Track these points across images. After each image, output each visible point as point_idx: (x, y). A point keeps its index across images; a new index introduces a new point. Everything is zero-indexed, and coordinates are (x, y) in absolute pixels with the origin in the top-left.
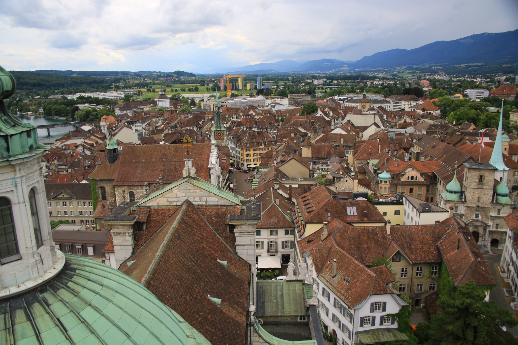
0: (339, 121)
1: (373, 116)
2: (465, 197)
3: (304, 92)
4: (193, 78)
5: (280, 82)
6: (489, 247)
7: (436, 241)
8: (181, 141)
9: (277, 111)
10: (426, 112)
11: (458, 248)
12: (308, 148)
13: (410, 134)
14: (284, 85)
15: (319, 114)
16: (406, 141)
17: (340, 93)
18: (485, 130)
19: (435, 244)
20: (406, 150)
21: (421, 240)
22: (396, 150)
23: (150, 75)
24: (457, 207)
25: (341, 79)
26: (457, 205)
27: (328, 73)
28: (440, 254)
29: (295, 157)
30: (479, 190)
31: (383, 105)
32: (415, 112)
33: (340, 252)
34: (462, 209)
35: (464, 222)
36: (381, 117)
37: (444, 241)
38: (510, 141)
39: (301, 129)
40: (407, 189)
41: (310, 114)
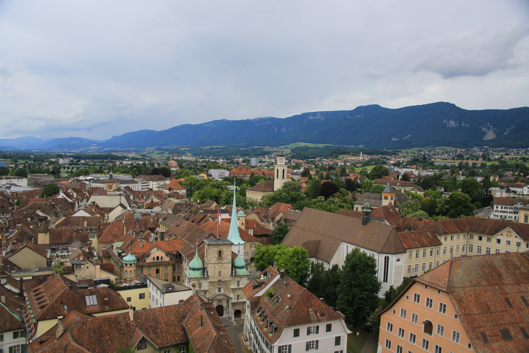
0: (83, 203)
1: (119, 197)
2: (207, 273)
3: (47, 171)
5: (20, 160)
6: (233, 319)
7: (181, 321)
9: (13, 193)
10: (172, 191)
11: (202, 325)
12: (45, 234)
13: (156, 214)
14: (24, 164)
15: (61, 195)
16: (152, 221)
17: (86, 173)
18: (225, 207)
19: (180, 324)
20: (152, 230)
21: (166, 322)
22: (142, 231)
24: (200, 284)
25: (89, 159)
26: (200, 282)
27: (75, 151)
28: (185, 335)
29: (28, 245)
30: (219, 264)
31: (129, 185)
32: (162, 192)
33: (78, 349)
34: (205, 286)
35: (207, 298)
36: (127, 198)
37: (188, 320)
38: (246, 217)
39: (39, 213)
40: (153, 270)
41: (50, 195)
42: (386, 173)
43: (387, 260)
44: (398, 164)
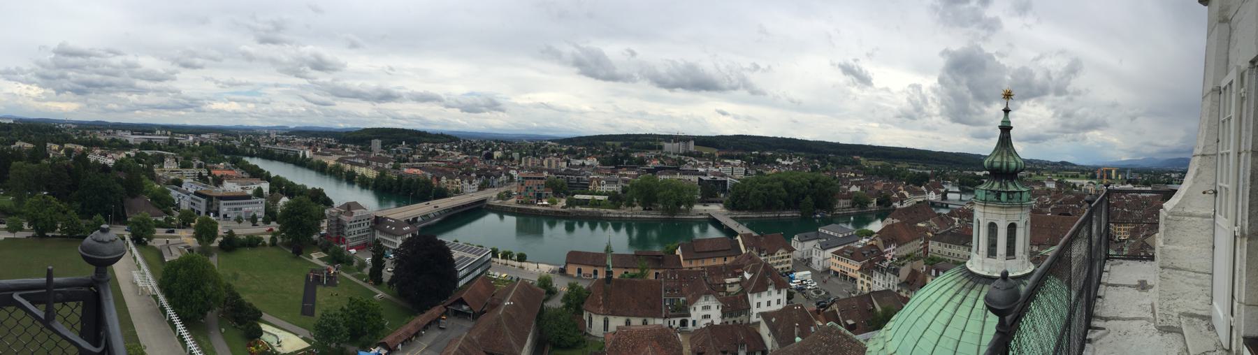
4: (1075, 167)
23: (1040, 163)
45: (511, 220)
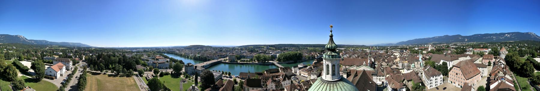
8: (363, 58)
15: (389, 53)
17: (393, 49)
42: (449, 47)
43: (449, 62)
44: (451, 45)
45: (227, 66)
